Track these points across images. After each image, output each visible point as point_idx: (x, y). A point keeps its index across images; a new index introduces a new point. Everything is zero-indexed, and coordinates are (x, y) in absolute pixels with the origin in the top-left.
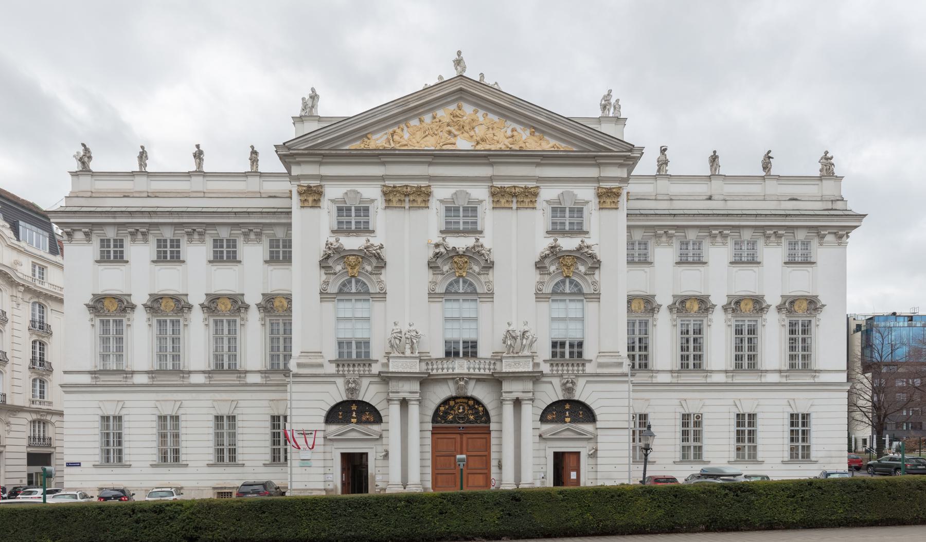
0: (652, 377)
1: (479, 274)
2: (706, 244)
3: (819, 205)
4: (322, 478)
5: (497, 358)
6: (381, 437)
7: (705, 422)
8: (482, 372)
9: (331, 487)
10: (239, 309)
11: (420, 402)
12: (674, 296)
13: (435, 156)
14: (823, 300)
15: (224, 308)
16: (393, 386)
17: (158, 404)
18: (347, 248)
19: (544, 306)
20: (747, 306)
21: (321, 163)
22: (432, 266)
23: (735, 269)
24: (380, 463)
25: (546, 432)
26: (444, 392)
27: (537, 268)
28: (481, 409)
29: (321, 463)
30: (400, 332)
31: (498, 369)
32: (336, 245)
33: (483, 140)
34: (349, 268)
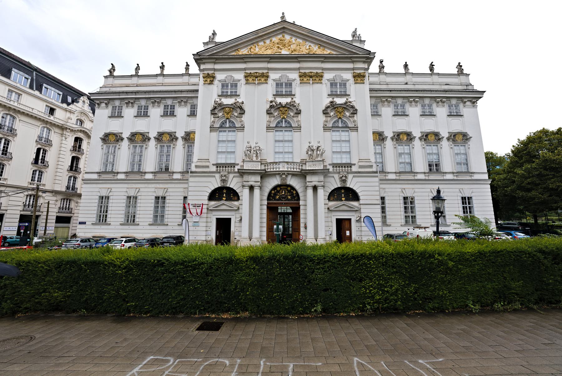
0: (385, 176)
1: (293, 117)
2: (407, 106)
3: (460, 88)
4: (204, 233)
5: (303, 162)
6: (239, 208)
7: (416, 202)
8: (295, 170)
9: (210, 239)
10: (172, 140)
11: (261, 188)
12: (393, 132)
13: (271, 58)
14: (470, 134)
15: (166, 138)
16: (246, 178)
17: (128, 190)
18: (225, 103)
19: (328, 134)
20: (432, 138)
21: (215, 63)
22: (269, 113)
23: (423, 118)
24: (238, 224)
25: (331, 207)
26: (275, 181)
27: (324, 113)
28: (294, 192)
29: (204, 224)
30: (251, 147)
31: (304, 168)
32: (219, 102)
33: (295, 50)
34: (226, 114)
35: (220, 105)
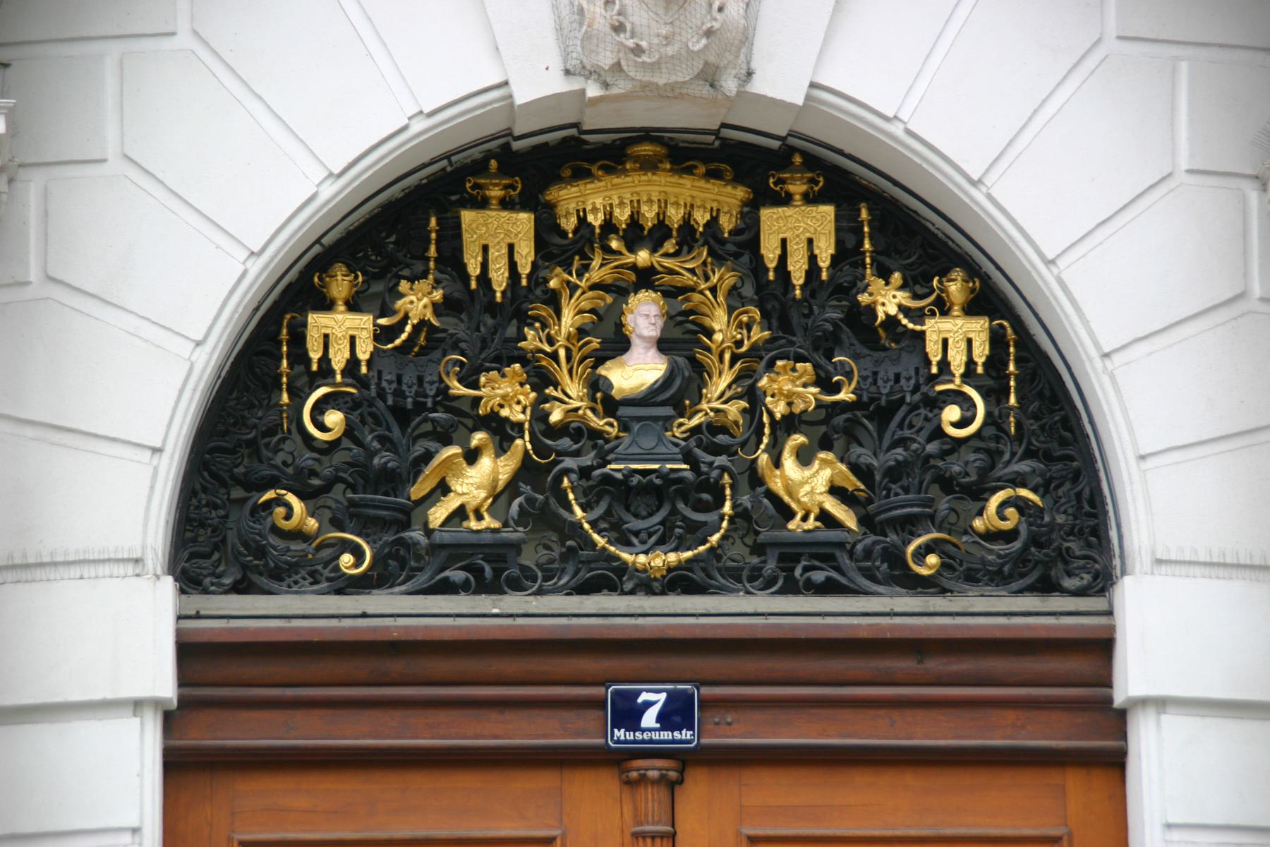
28: (957, 337)
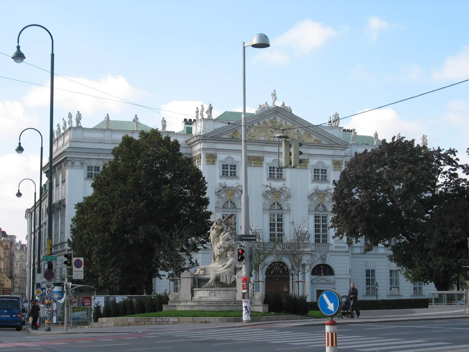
1: (284, 200)
27: (308, 198)
35: (225, 187)
